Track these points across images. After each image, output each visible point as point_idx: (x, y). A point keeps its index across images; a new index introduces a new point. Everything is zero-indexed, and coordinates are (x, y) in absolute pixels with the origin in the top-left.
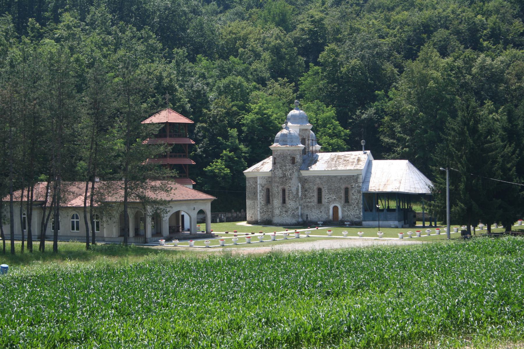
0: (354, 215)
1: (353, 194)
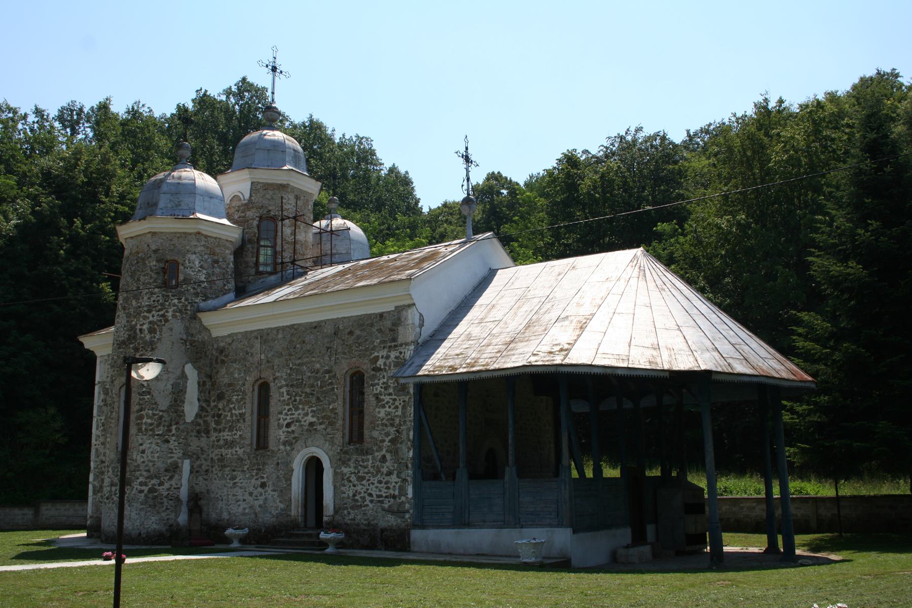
0: (380, 500)
1: (377, 397)
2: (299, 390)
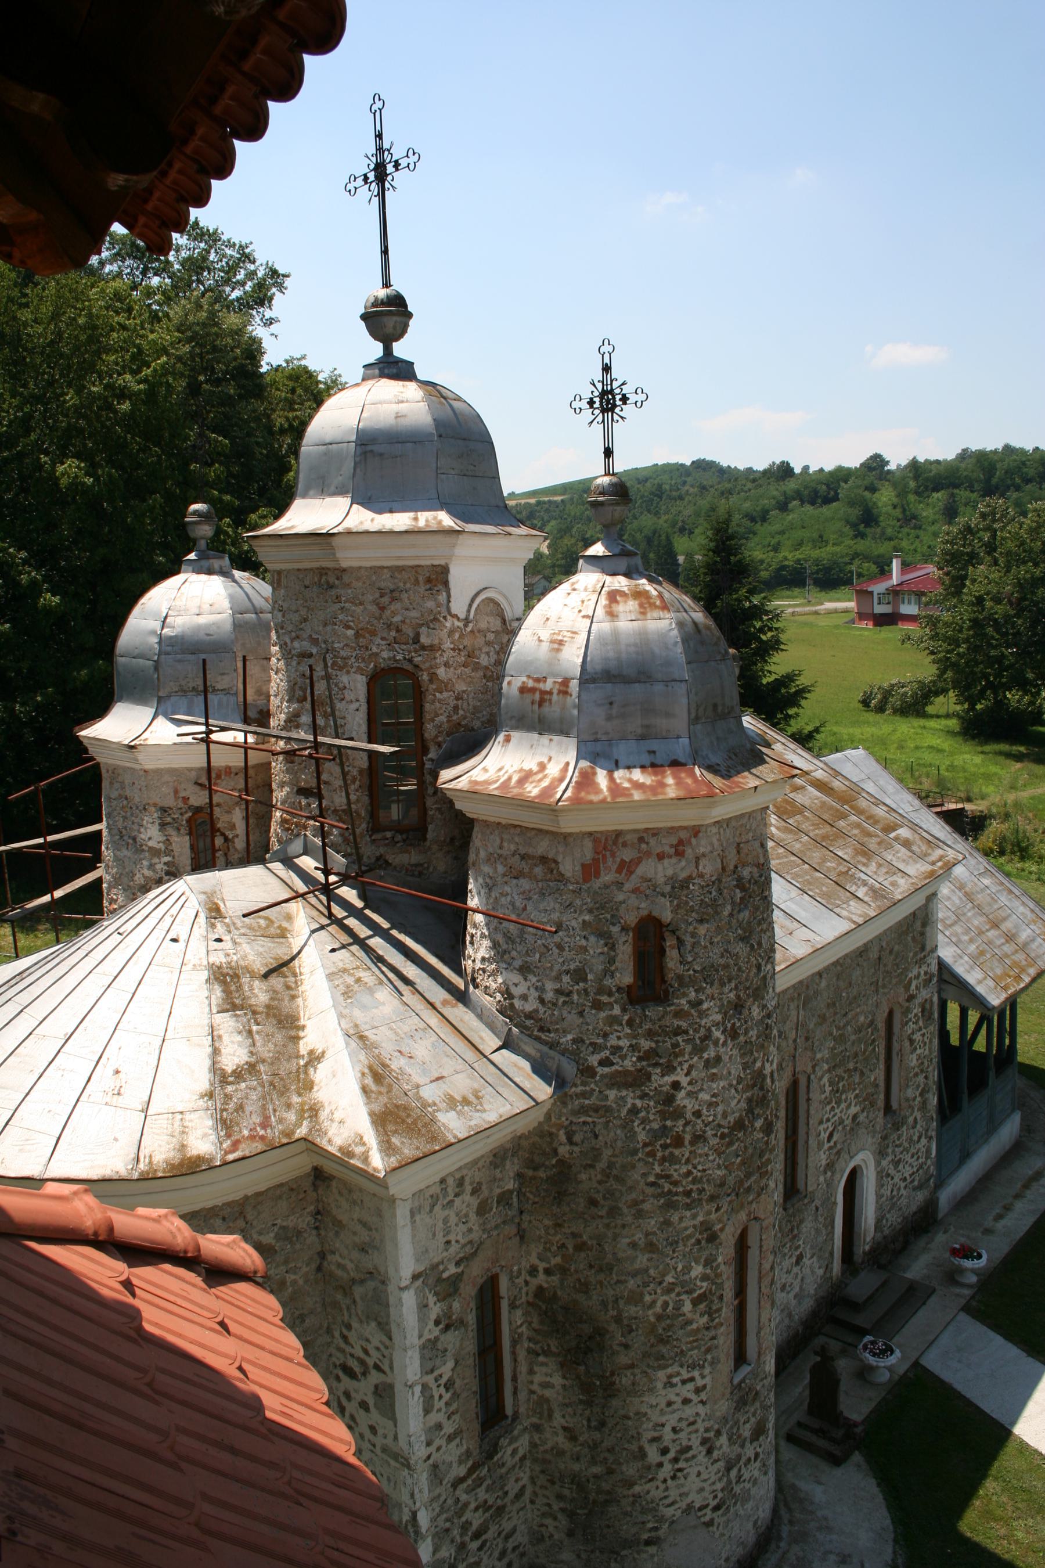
2: (840, 1071)
